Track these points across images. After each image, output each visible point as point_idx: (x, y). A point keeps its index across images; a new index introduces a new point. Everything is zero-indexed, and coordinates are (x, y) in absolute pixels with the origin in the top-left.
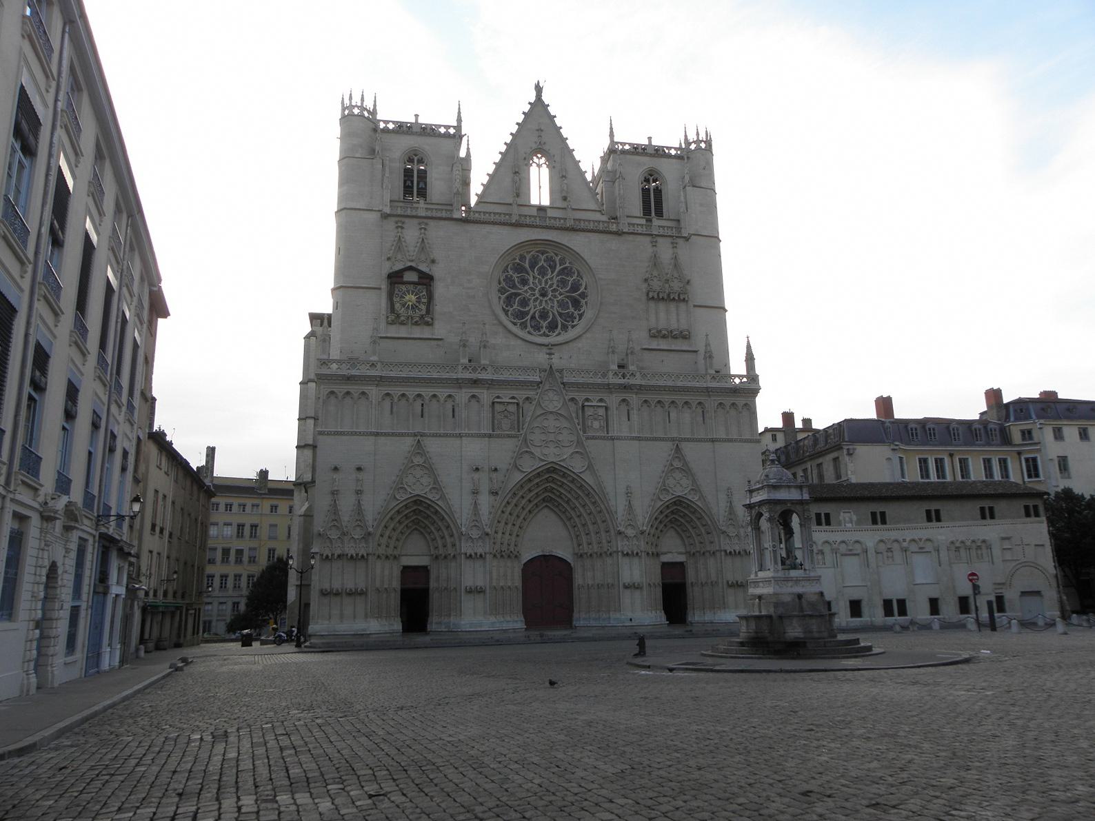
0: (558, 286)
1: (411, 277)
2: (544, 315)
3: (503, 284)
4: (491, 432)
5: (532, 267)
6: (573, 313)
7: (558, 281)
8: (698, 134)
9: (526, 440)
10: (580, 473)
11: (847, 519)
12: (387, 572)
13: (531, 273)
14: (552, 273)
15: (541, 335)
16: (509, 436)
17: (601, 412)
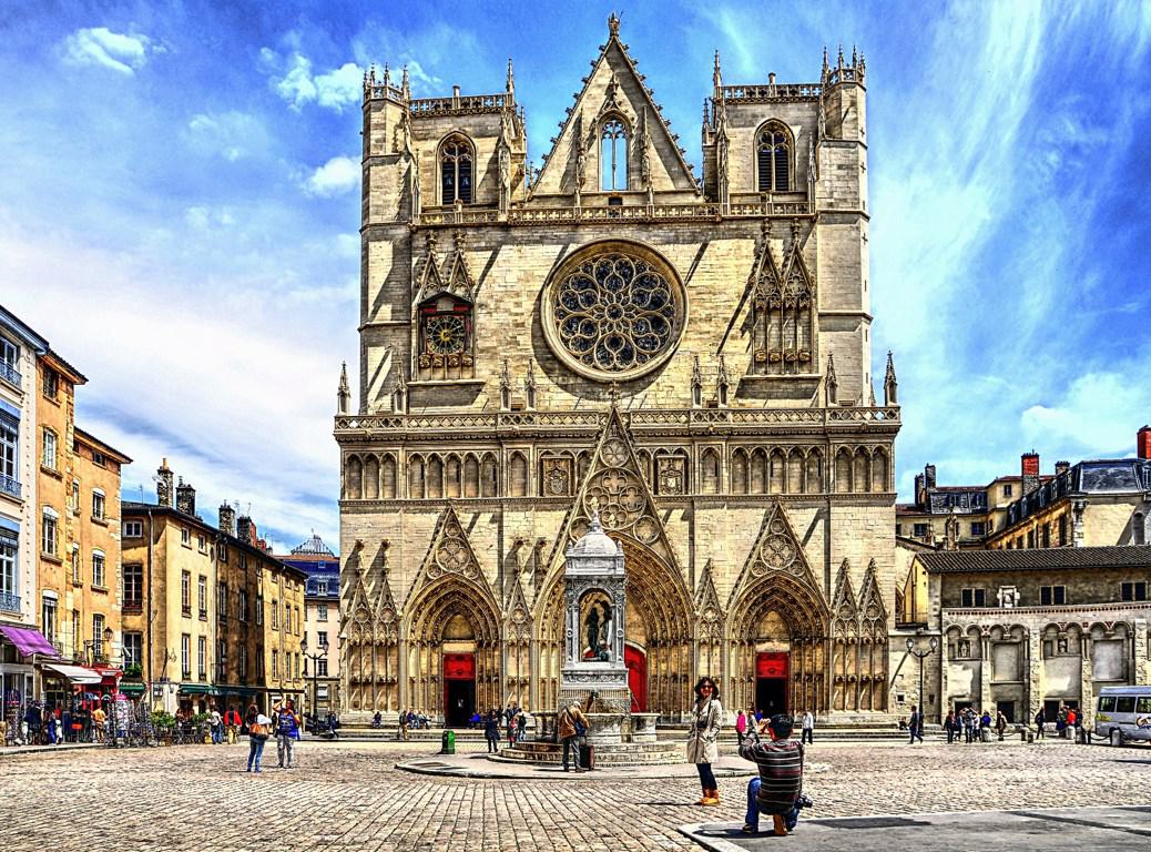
0: (634, 302)
1: (443, 306)
2: (615, 342)
3: (562, 306)
4: (538, 497)
5: (601, 275)
6: (653, 338)
7: (634, 294)
8: (840, 60)
9: (581, 506)
10: (650, 545)
11: (1008, 598)
12: (424, 660)
13: (599, 287)
14: (627, 284)
15: (610, 370)
16: (561, 501)
17: (679, 466)
